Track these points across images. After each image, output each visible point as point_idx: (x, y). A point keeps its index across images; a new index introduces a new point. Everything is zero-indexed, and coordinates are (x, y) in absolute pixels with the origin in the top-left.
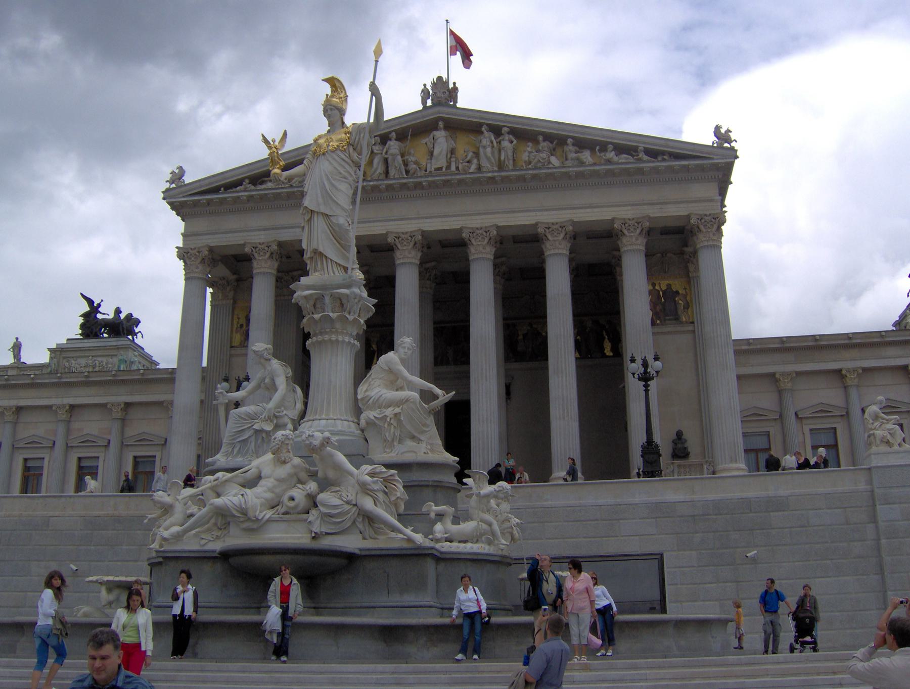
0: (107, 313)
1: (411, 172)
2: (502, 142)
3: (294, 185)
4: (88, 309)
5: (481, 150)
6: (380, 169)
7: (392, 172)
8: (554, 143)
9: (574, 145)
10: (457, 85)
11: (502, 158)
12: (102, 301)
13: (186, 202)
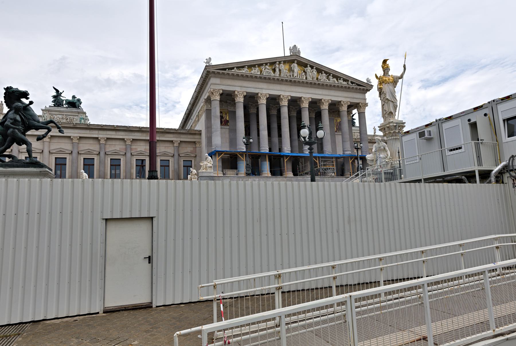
0: (67, 96)
1: (287, 76)
2: (313, 71)
3: (252, 73)
4: (54, 93)
5: (308, 73)
6: (278, 73)
7: (282, 75)
8: (328, 75)
9: (332, 76)
10: (300, 49)
11: (314, 77)
12: (63, 91)
13: (214, 72)
